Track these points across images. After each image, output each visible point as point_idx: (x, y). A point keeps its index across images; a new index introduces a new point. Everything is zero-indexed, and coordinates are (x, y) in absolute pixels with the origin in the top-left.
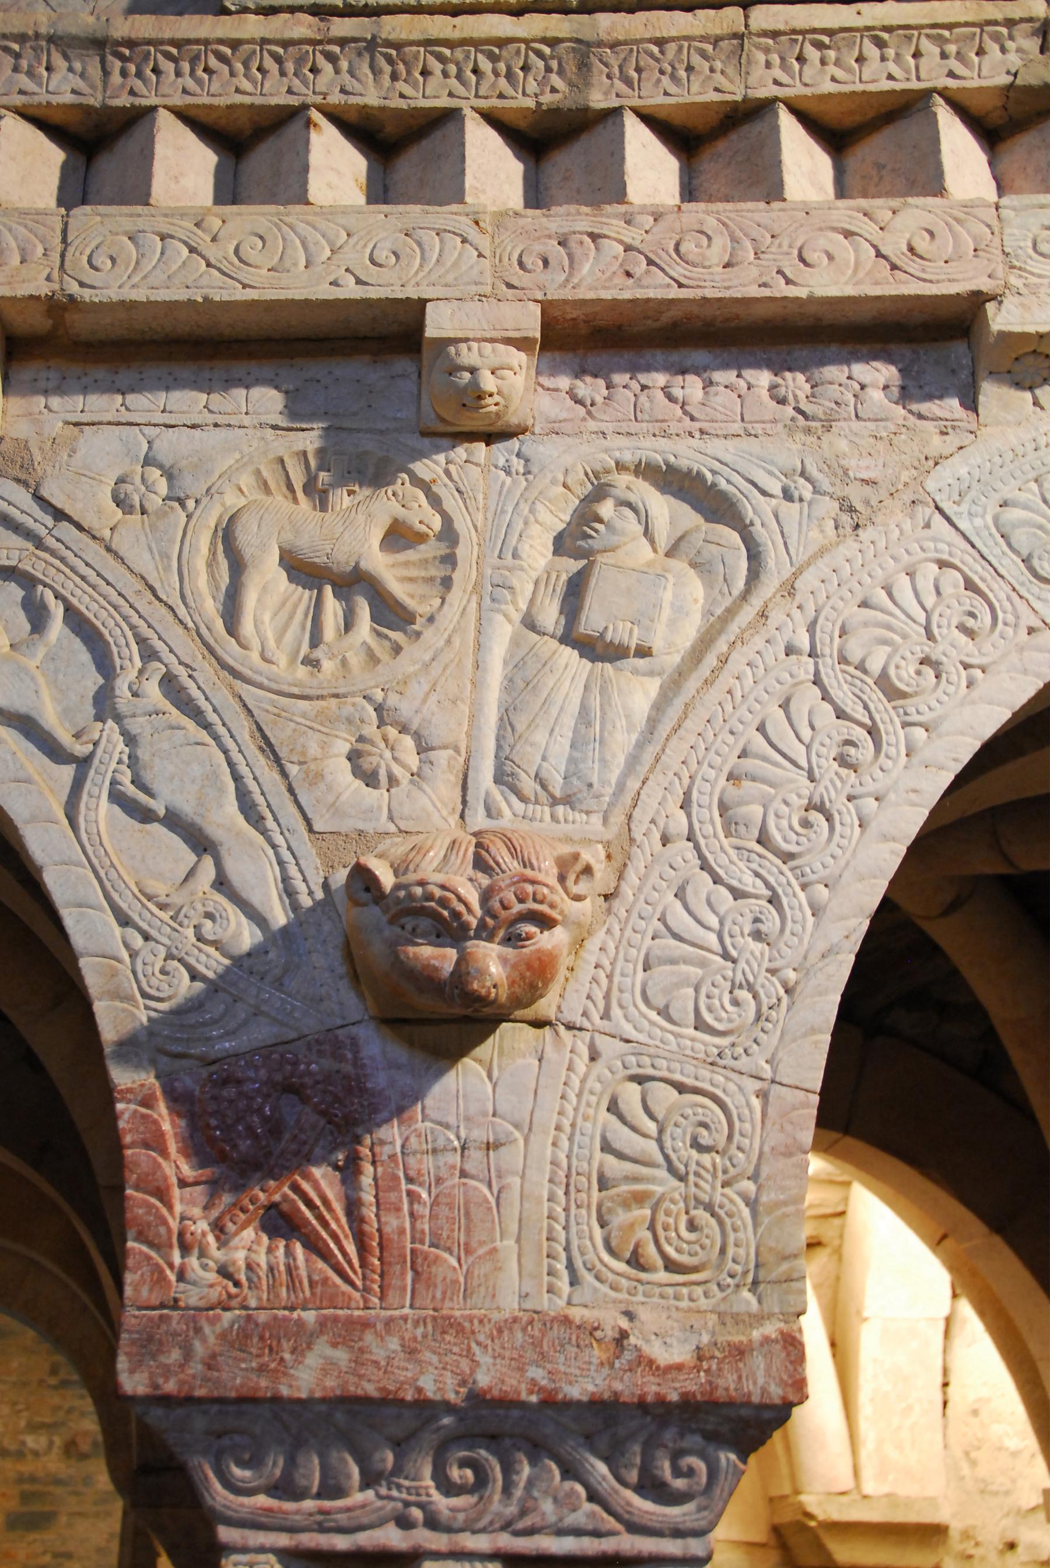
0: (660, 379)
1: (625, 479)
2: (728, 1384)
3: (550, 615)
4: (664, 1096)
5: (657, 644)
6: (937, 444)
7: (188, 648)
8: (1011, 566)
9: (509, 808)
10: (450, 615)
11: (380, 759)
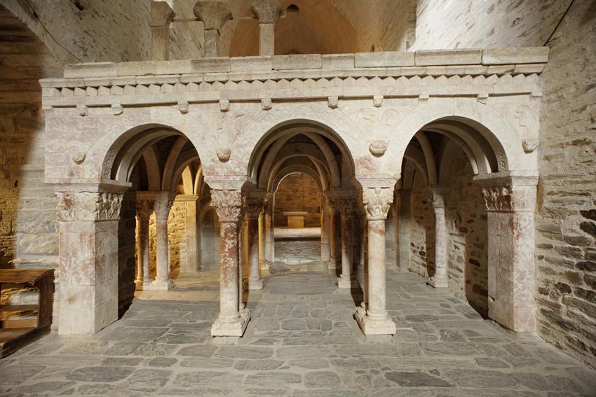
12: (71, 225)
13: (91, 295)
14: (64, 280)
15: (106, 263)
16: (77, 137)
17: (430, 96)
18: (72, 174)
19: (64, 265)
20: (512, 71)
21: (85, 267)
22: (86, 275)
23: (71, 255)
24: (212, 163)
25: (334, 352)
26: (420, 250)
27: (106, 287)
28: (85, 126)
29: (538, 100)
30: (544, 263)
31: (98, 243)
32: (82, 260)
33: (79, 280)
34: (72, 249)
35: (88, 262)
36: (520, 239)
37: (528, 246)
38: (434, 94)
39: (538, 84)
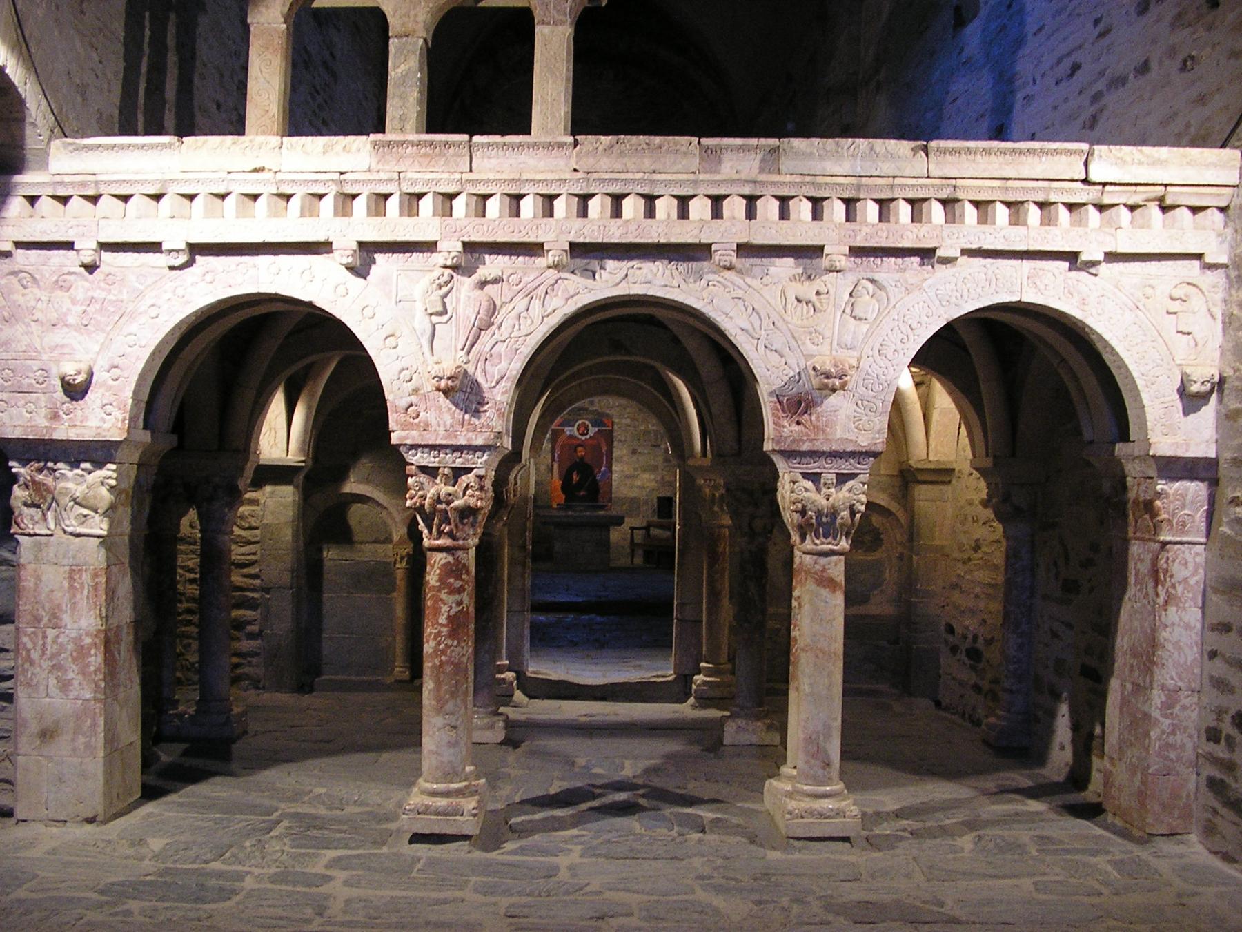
0: (872, 259)
1: (864, 281)
2: (873, 448)
3: (848, 310)
4: (865, 403)
5: (868, 317)
6: (927, 276)
7: (777, 316)
8: (937, 303)
9: (840, 350)
10: (828, 310)
11: (816, 341)
12: (47, 544)
13: (94, 725)
14: (29, 685)
15: (123, 648)
16: (71, 320)
17: (968, 252)
18: (55, 416)
19: (30, 645)
20: (1161, 199)
21: (81, 653)
22: (83, 672)
23: (46, 619)
24: (414, 399)
25: (706, 871)
26: (968, 644)
27: (121, 708)
28: (90, 294)
29: (1221, 271)
30: (1219, 668)
31: (111, 593)
32: (74, 635)
33: (65, 686)
34: (47, 606)
35: (88, 640)
36: (1172, 609)
37: (1188, 627)
38: (974, 246)
39: (1219, 235)
